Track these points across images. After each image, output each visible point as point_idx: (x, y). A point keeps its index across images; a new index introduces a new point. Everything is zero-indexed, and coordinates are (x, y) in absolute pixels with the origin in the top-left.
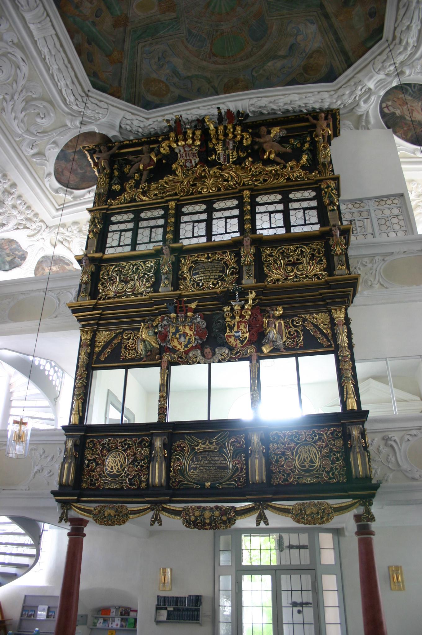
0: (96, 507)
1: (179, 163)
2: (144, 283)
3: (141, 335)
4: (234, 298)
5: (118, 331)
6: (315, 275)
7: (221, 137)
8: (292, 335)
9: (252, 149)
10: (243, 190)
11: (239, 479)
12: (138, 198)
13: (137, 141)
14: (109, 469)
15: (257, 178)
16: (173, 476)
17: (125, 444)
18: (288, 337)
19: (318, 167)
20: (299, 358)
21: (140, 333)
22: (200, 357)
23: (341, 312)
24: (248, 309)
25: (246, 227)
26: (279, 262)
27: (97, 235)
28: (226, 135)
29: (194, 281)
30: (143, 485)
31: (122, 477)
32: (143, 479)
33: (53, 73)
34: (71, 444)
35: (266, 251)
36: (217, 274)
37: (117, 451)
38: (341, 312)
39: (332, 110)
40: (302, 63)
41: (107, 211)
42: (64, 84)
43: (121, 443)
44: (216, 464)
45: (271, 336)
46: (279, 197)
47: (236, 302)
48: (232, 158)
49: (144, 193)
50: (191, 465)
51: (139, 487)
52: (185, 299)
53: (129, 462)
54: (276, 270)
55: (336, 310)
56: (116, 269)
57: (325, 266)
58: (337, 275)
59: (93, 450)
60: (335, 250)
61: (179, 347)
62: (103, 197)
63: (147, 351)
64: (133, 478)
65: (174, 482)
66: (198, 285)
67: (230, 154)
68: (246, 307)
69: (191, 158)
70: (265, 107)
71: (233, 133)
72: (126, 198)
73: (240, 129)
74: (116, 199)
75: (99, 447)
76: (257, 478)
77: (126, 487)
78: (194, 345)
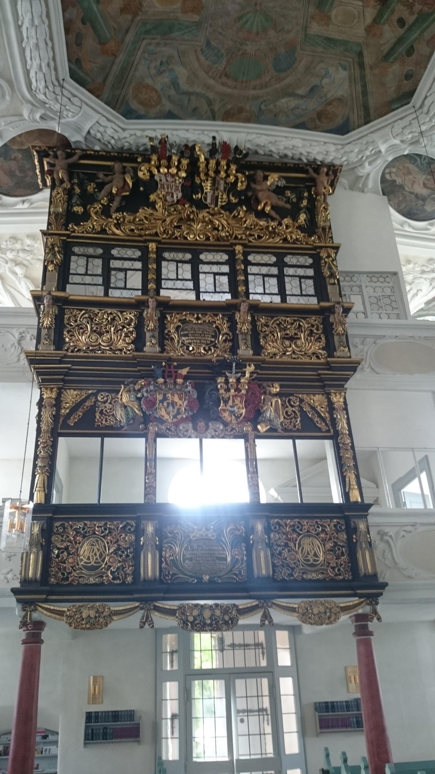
0: (70, 607)
1: (159, 195)
2: (122, 337)
3: (121, 399)
4: (230, 368)
5: (90, 392)
6: (314, 354)
7: (211, 173)
8: (289, 416)
9: (246, 196)
10: (236, 244)
11: (240, 572)
12: (110, 229)
13: (104, 153)
14: (85, 560)
15: (252, 233)
16: (165, 569)
17: (105, 529)
18: (284, 418)
19: (316, 230)
20: (297, 441)
21: (119, 396)
22: (191, 431)
23: (340, 397)
24: (244, 383)
25: (240, 289)
26: (275, 335)
27: (57, 267)
28: (217, 172)
29: (182, 343)
30: (129, 579)
31: (102, 569)
32: (128, 572)
34: (38, 529)
35: (261, 319)
36: (209, 339)
37: (94, 537)
38: (340, 397)
39: (334, 166)
41: (67, 238)
43: (101, 527)
44: (214, 554)
45: (268, 415)
46: (274, 259)
47: (231, 373)
48: (221, 202)
49: (118, 226)
50: (185, 555)
51: (124, 582)
52: (175, 364)
53: (110, 551)
54: (273, 342)
55: (335, 393)
56: (87, 315)
57: (324, 345)
58: (338, 357)
59: (62, 536)
60: (337, 330)
61: (166, 417)
62: (61, 219)
63: (128, 418)
64: (117, 570)
65: (166, 575)
66: (188, 348)
67: (220, 197)
68: (242, 380)
69: (173, 191)
70: (264, 146)
71: (226, 172)
72: (96, 227)
73: (234, 168)
74: (80, 225)
75: (72, 533)
76: (264, 572)
77: (107, 582)
78: (184, 416)
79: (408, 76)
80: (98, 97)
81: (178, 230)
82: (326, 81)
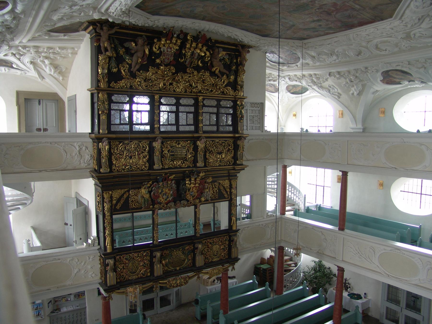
48: (194, 64)
67: (194, 62)
78: (170, 199)
81: (171, 86)
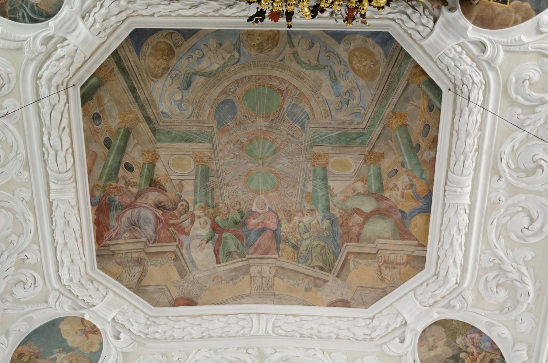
33: (478, 131)
40: (175, 62)
42: (472, 117)
79: (97, 118)
80: (418, 66)
82: (178, 97)
